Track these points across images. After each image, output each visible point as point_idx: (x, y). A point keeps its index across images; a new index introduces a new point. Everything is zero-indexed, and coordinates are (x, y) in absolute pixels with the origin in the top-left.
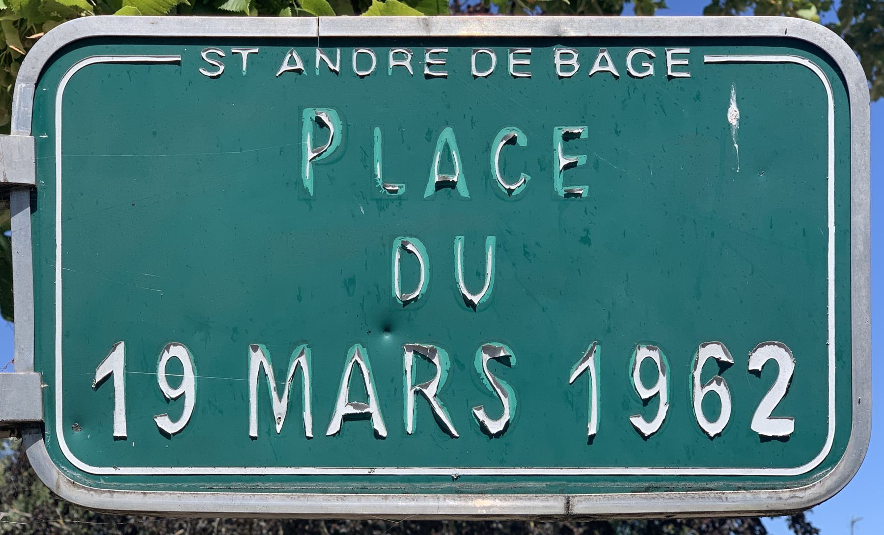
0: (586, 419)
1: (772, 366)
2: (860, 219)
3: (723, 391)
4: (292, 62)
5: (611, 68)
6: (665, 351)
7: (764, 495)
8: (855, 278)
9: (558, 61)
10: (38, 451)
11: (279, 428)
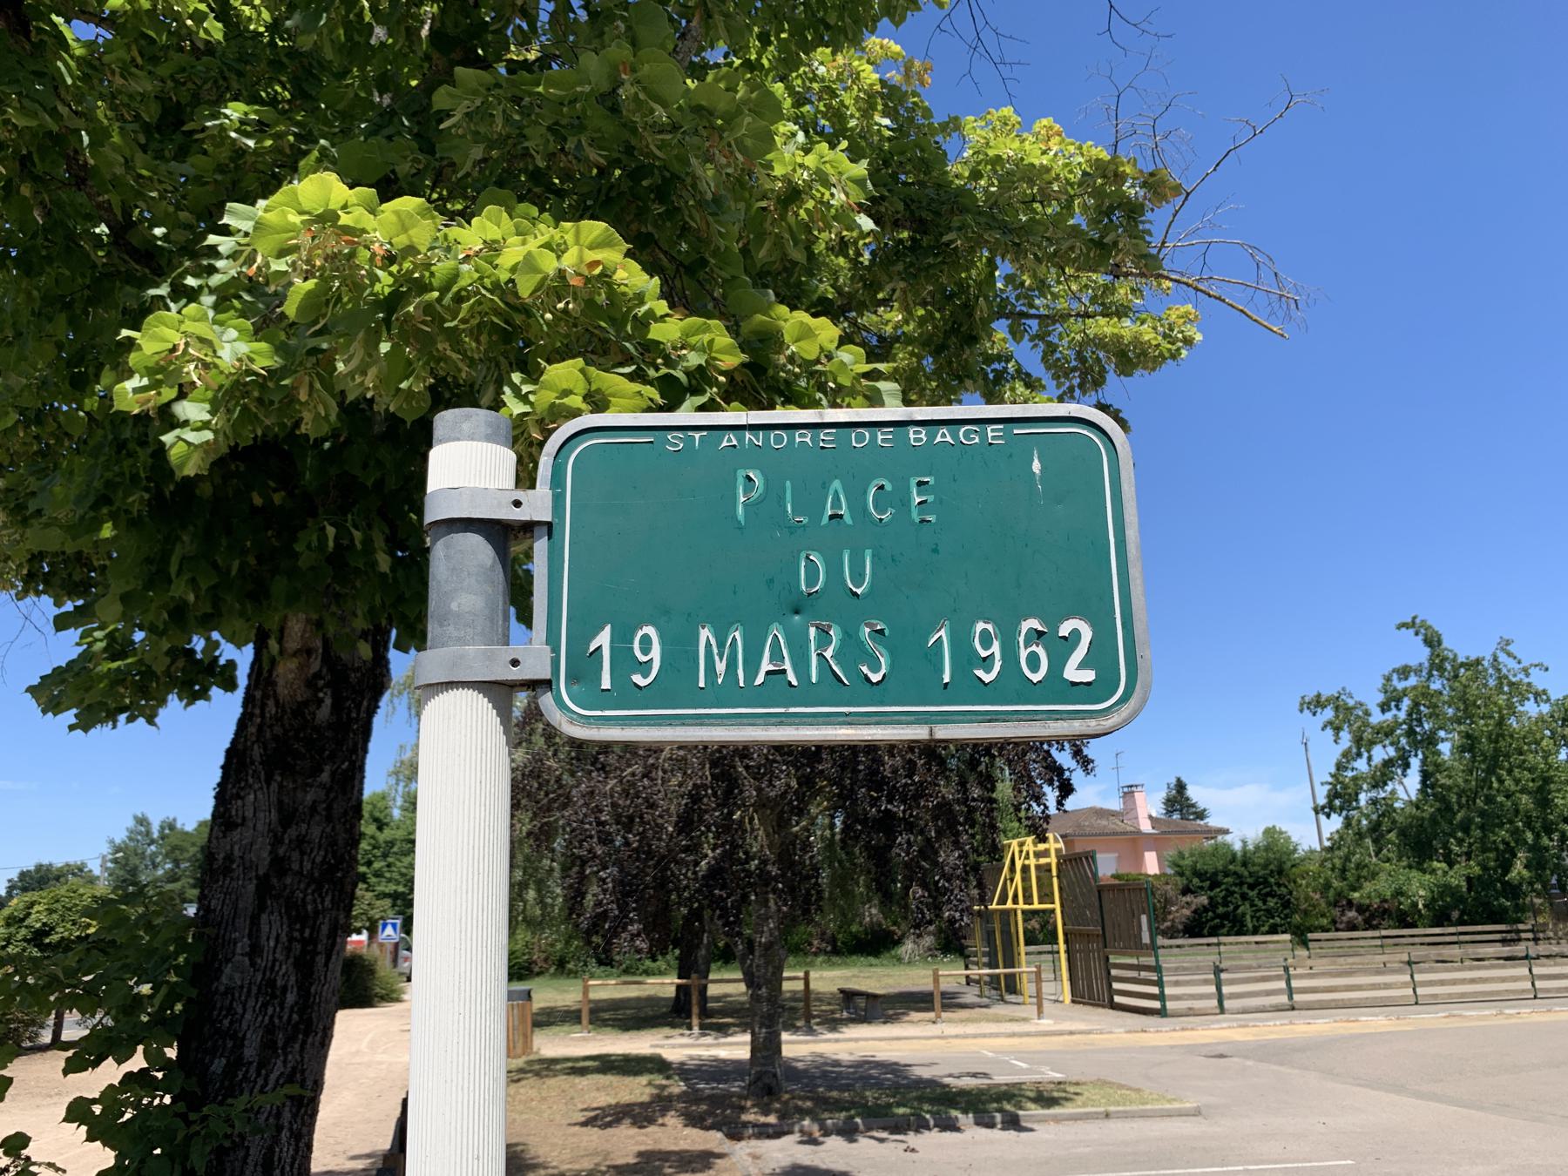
0: (941, 671)
1: (1076, 634)
2: (1132, 534)
3: (1041, 651)
4: (729, 440)
5: (949, 439)
6: (996, 624)
7: (1076, 724)
8: (1131, 571)
9: (912, 436)
10: (546, 701)
11: (720, 681)
